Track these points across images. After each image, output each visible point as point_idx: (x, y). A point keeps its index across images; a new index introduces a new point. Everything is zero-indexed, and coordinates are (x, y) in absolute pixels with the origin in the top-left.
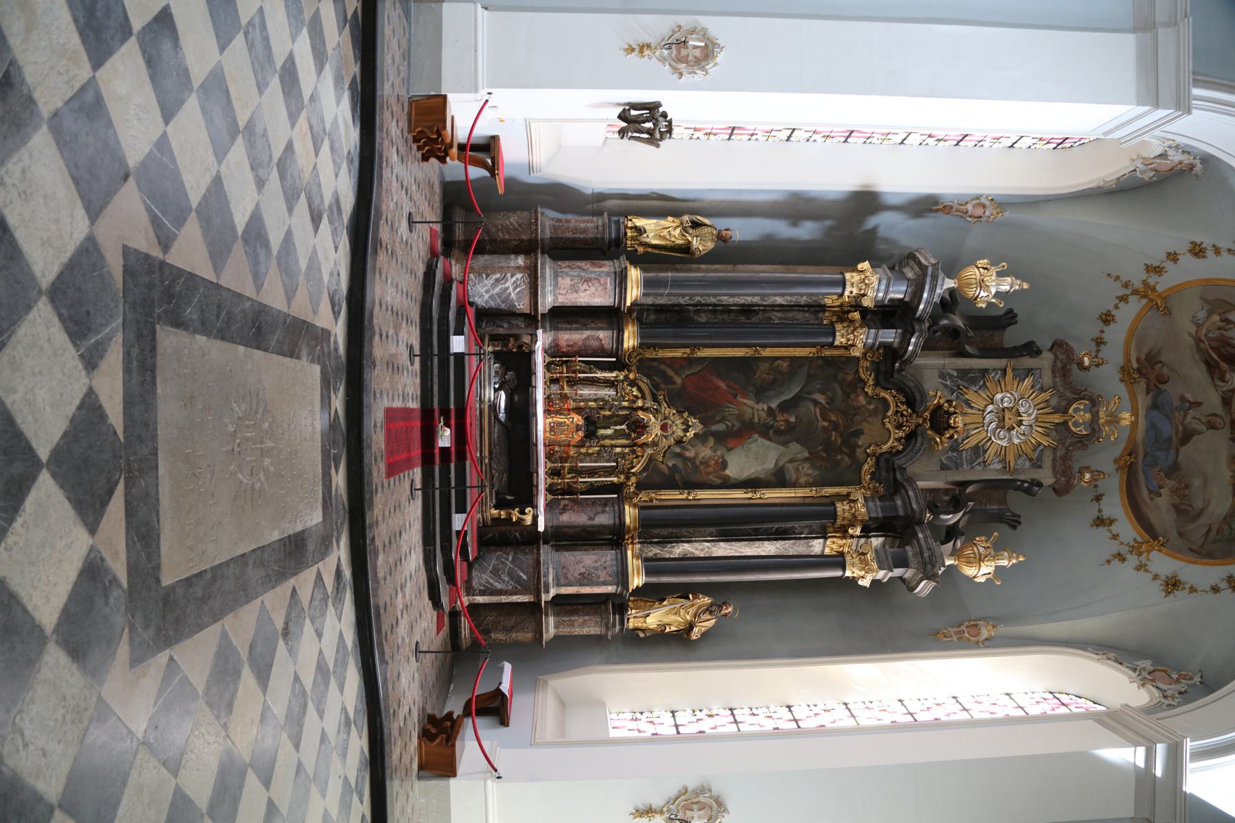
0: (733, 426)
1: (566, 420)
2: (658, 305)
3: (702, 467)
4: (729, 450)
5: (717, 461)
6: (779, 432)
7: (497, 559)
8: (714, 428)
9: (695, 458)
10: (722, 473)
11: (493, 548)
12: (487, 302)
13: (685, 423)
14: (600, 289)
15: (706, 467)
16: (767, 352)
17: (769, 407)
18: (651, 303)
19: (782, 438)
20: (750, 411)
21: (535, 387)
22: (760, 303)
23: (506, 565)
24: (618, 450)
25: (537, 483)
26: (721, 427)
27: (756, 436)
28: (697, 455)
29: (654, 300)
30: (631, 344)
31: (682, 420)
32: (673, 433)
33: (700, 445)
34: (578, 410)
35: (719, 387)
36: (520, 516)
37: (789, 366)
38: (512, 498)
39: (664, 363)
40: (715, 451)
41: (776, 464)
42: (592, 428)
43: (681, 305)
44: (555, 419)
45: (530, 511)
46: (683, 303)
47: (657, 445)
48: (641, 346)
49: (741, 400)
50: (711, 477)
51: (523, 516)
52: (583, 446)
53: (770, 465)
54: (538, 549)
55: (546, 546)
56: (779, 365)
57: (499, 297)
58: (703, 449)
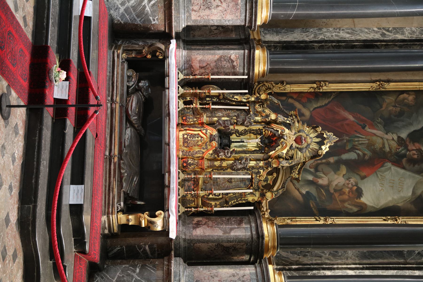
0: (364, 155)
1: (200, 133)
2: (285, 42)
3: (336, 195)
4: (363, 178)
5: (351, 189)
6: (412, 161)
7: (122, 271)
8: (345, 156)
9: (328, 186)
10: (358, 201)
11: (119, 261)
12: (123, 15)
13: (320, 136)
14: (231, 5)
15: (341, 195)
16: (391, 86)
17: (399, 137)
18: (278, 40)
19: (416, 166)
20: (379, 141)
21: (168, 88)
22: (382, 38)
23: (133, 277)
24: (252, 163)
25: (169, 182)
26: (352, 156)
27: (389, 165)
28: (330, 183)
29: (281, 38)
30: (261, 70)
31: (316, 134)
32: (308, 145)
33: (333, 173)
34: (211, 124)
35: (345, 119)
36: (149, 218)
37: (415, 99)
38: (142, 203)
39: (292, 98)
40: (348, 179)
41: (414, 193)
42: (225, 141)
43: (305, 42)
44: (188, 132)
45: (161, 214)
46: (307, 39)
47: (292, 158)
48: (271, 71)
49: (369, 130)
50: (346, 205)
51: (153, 219)
52: (215, 160)
53: (407, 193)
54: (169, 261)
55: (178, 259)
56: (404, 99)
57: (134, 11)
58: (336, 176)
